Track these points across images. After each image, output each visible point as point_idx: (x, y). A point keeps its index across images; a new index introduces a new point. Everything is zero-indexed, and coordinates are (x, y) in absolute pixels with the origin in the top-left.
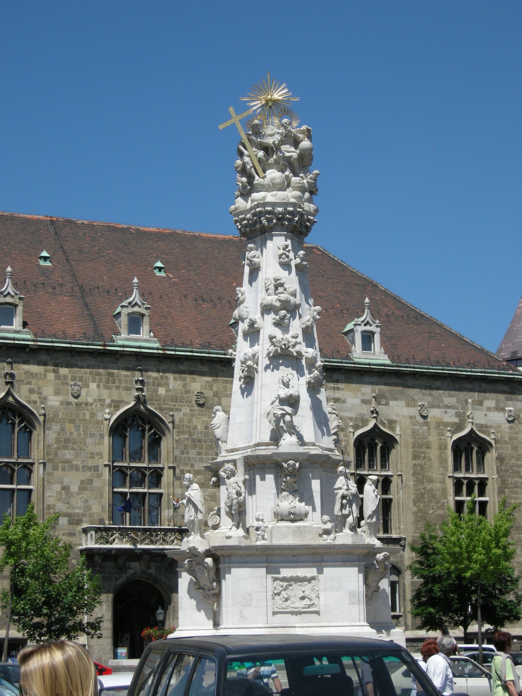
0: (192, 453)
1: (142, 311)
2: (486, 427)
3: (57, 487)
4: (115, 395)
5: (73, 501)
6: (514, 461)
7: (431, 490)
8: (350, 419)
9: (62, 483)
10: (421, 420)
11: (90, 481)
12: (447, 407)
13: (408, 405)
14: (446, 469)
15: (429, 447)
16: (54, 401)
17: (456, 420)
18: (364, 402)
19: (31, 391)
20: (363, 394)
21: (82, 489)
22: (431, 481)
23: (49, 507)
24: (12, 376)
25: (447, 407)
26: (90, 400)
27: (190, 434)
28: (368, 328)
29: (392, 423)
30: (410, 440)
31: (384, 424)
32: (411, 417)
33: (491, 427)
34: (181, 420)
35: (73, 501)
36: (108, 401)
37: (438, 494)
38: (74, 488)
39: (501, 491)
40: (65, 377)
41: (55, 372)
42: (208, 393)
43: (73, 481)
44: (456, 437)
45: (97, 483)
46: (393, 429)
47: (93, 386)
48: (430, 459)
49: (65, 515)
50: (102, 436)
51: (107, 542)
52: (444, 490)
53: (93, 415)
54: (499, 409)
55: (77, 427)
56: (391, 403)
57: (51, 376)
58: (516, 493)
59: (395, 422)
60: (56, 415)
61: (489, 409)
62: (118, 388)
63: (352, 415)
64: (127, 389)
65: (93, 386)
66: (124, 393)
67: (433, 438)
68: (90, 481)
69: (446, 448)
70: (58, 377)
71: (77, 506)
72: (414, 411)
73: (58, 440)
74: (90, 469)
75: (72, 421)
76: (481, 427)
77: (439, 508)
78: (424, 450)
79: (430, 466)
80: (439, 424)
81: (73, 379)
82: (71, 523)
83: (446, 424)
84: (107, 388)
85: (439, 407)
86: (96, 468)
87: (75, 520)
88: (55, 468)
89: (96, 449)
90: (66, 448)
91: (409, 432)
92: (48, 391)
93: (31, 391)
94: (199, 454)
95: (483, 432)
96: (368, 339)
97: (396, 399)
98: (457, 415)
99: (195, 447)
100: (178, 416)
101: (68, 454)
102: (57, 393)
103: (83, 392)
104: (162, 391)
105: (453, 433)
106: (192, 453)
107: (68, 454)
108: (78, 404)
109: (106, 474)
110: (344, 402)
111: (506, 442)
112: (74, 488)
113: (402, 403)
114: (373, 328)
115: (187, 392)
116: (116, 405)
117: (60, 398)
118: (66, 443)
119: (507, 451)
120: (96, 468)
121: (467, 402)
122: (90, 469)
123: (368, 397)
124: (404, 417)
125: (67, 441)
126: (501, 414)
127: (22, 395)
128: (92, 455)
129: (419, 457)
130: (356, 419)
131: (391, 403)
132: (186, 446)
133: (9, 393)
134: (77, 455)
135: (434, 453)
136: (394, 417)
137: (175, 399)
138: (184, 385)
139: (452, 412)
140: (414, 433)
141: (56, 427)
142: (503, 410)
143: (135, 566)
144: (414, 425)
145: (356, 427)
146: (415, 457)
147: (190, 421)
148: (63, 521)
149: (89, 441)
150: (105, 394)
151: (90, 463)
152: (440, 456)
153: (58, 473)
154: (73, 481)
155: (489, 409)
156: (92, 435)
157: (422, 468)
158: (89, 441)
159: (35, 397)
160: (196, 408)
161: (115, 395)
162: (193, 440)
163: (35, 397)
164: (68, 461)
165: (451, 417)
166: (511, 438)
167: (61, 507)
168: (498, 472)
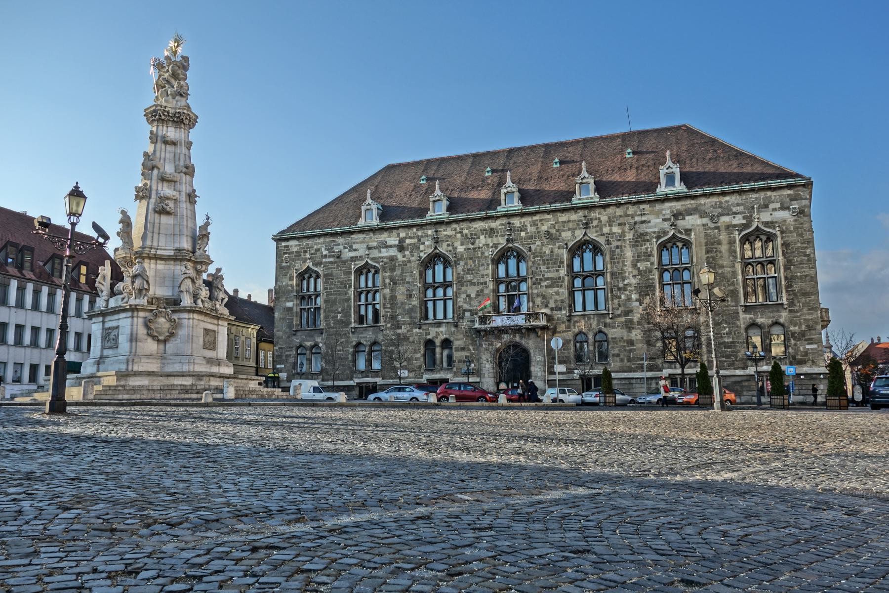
0: (543, 268)
1: (513, 190)
2: (772, 222)
3: (464, 296)
4: (495, 240)
5: (472, 303)
6: (799, 245)
7: (722, 273)
8: (654, 233)
9: (465, 292)
10: (712, 225)
11: (482, 291)
12: (736, 213)
13: (701, 217)
14: (736, 257)
15: (719, 243)
16: (461, 249)
17: (744, 222)
18: (665, 220)
19: (448, 245)
20: (664, 215)
21: (478, 295)
22: (722, 267)
23: (460, 307)
24: (438, 238)
25: (736, 213)
26: (481, 245)
27: (542, 257)
28: (670, 171)
29: (688, 231)
30: (703, 241)
31: (681, 233)
32: (704, 225)
33: (776, 222)
34: (536, 249)
35: (472, 303)
36: (491, 245)
37: (729, 275)
38: (473, 295)
39: (787, 268)
40: (466, 235)
41: (461, 232)
42: (553, 231)
43: (473, 291)
44: (744, 233)
45: (486, 291)
46: (689, 235)
47: (482, 237)
48: (721, 252)
49: (469, 311)
50: (488, 265)
51: (485, 323)
52: (734, 273)
53: (483, 253)
54: (783, 208)
55: (474, 262)
56: (687, 218)
57: (459, 235)
58: (803, 268)
59: (690, 230)
60: (462, 256)
61: (774, 210)
62: (496, 236)
63: (656, 230)
64: (502, 236)
65: (482, 237)
66: (500, 238)
67: (723, 237)
68: (482, 291)
69: (735, 242)
70: (462, 236)
71: (475, 305)
72: (705, 220)
73: (463, 270)
74: (482, 284)
75: (471, 259)
76: (767, 224)
77: (729, 285)
78: (716, 246)
79: (721, 257)
80: (728, 227)
81: (471, 235)
82: (472, 315)
83: (735, 226)
84: (490, 237)
85: (728, 214)
86: (485, 283)
87: (473, 313)
88: (463, 285)
89: (486, 272)
90: (468, 274)
91: (702, 235)
92: (457, 244)
93: (448, 245)
94: (547, 268)
95: (769, 227)
96: (670, 179)
97: (691, 214)
98: (744, 218)
99: (545, 264)
100: (533, 247)
101: (469, 277)
102: (462, 244)
103: (477, 241)
104: (523, 234)
105: (740, 232)
106: (543, 268)
107: (469, 277)
108: (474, 249)
109: (491, 286)
110: (649, 222)
111: (791, 232)
112: (473, 295)
113: (696, 216)
114: (674, 170)
115: (539, 232)
116: (496, 246)
117: (464, 247)
118: (468, 271)
119: (792, 238)
120: (485, 283)
121: (753, 208)
122: (482, 284)
123: (667, 217)
124: (698, 225)
125: (469, 270)
126: (787, 212)
127: (443, 249)
128: (483, 276)
129: (712, 251)
130: (659, 232)
131: (687, 218)
132: (539, 265)
133: (436, 248)
134: (474, 277)
135: (724, 248)
136: (689, 227)
137: (531, 237)
138: (537, 229)
139: (740, 216)
140: (706, 235)
141: (462, 263)
142: (788, 208)
143: (506, 338)
144: (706, 230)
145: (658, 238)
146: (707, 252)
147: (541, 249)
148: (468, 314)
149: (481, 268)
150: (489, 241)
151: (482, 280)
152: (730, 248)
153: (464, 288)
154: (473, 291)
155: (774, 210)
156: (483, 265)
157: (714, 258)
158: (481, 268)
159: (450, 248)
160: (545, 241)
161: (495, 240)
162: (544, 260)
163: (450, 248)
164: (469, 281)
165: (739, 220)
166: (796, 228)
167: (466, 306)
168: (784, 254)
